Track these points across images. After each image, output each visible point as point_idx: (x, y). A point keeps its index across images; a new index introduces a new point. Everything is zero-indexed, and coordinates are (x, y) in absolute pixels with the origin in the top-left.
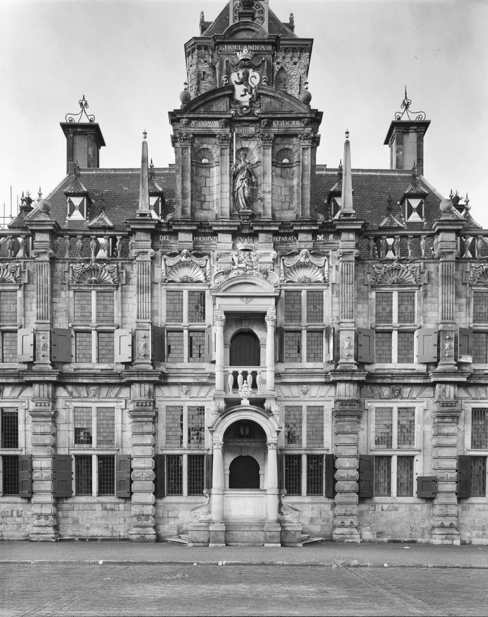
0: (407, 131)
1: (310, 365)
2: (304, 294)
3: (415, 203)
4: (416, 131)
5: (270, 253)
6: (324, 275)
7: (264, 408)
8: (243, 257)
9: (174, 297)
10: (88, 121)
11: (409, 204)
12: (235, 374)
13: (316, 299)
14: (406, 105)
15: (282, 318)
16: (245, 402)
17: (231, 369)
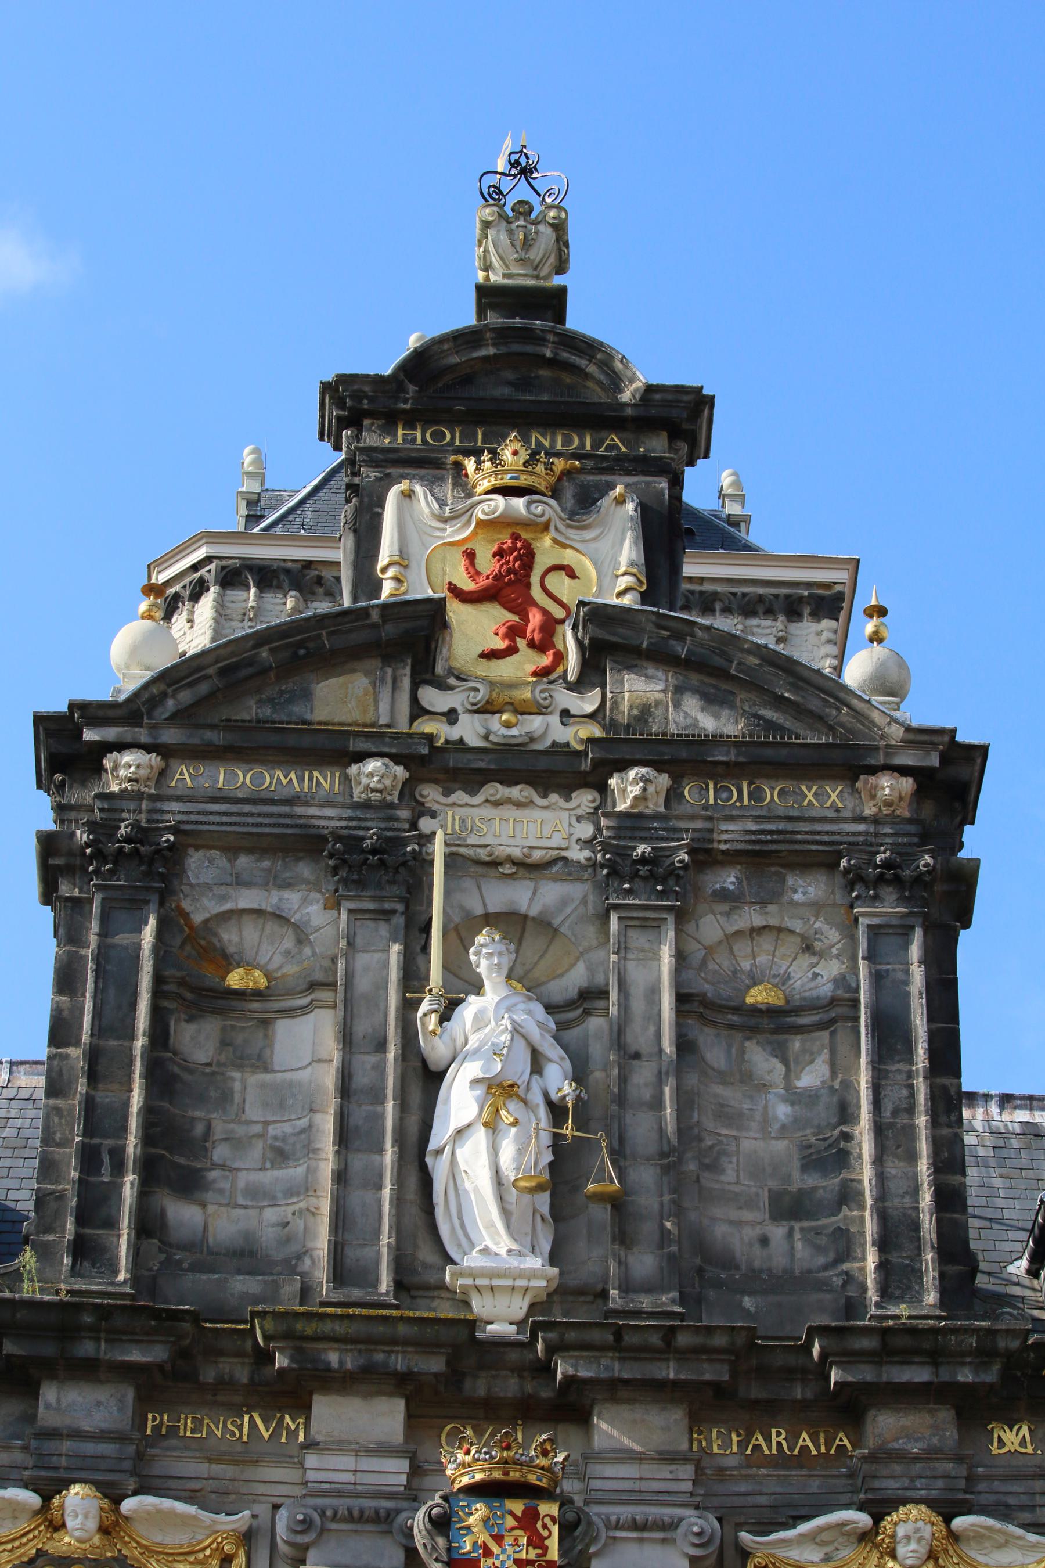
5: (672, 1525)
8: (483, 1537)
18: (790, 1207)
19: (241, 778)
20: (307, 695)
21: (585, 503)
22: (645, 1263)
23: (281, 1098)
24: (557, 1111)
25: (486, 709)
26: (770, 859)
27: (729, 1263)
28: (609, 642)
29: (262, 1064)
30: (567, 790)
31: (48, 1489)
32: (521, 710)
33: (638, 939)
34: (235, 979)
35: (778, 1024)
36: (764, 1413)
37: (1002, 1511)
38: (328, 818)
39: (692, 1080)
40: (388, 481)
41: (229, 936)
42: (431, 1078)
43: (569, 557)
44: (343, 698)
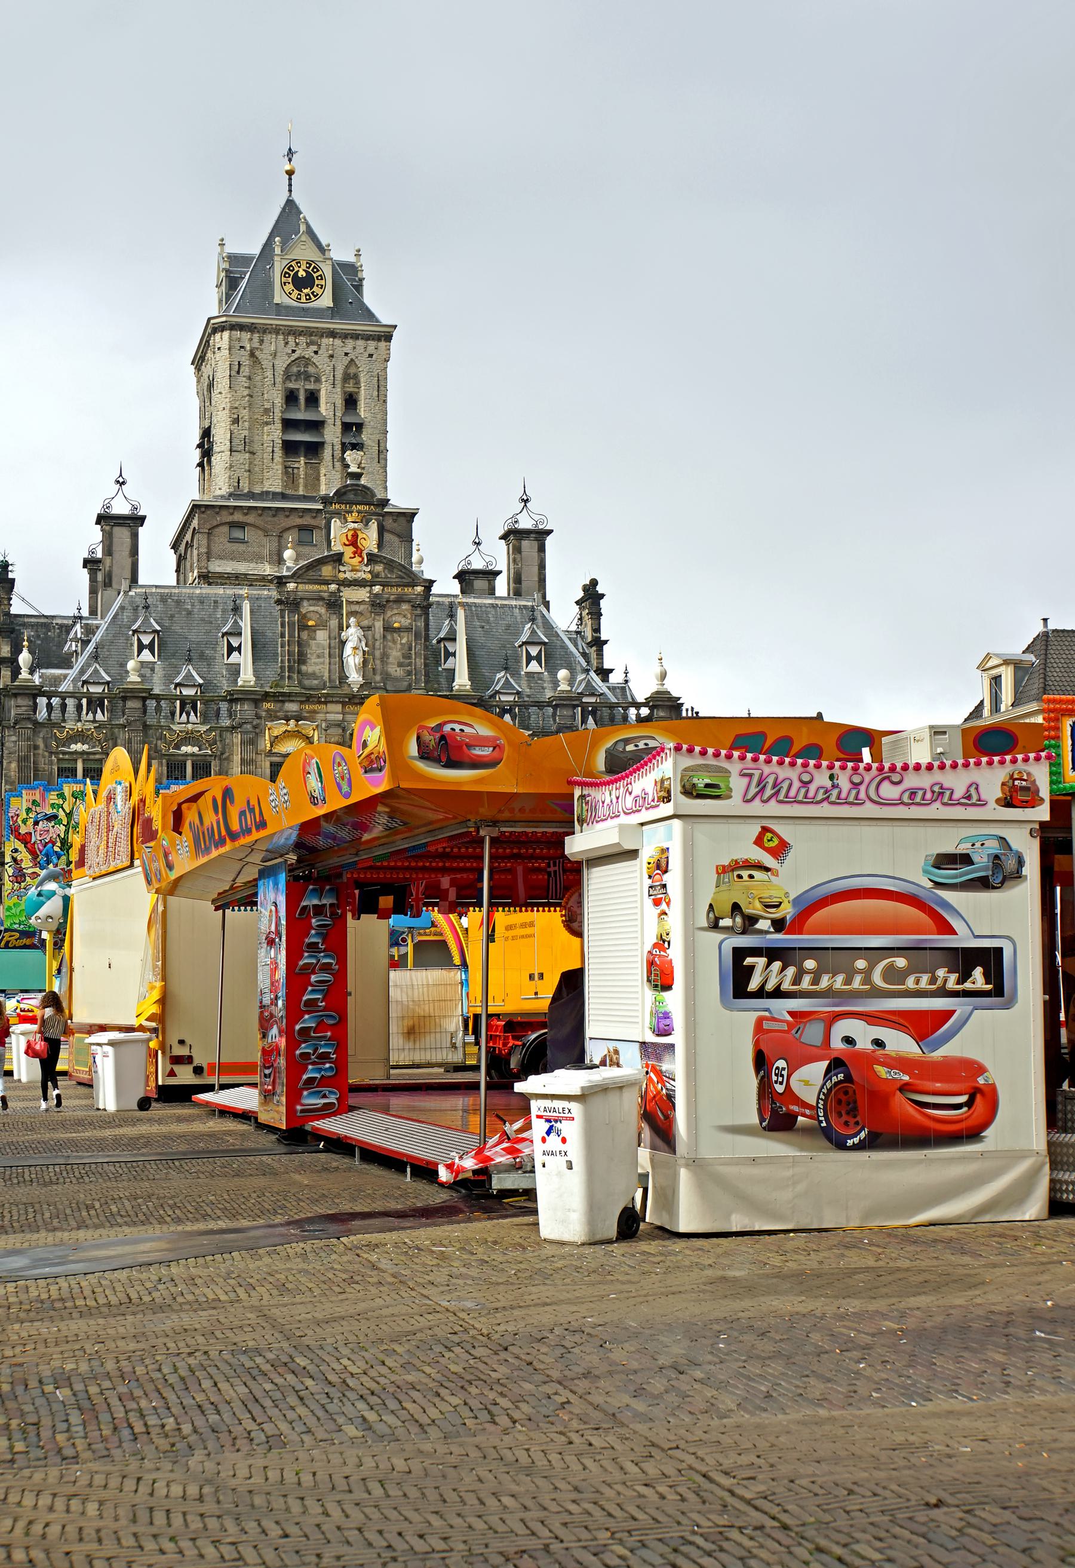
0: (527, 541)
3: (534, 651)
4: (536, 539)
11: (527, 650)
14: (526, 501)
18: (400, 665)
19: (310, 587)
20: (320, 570)
21: (367, 525)
22: (378, 678)
23: (318, 645)
26: (399, 600)
28: (372, 559)
30: (365, 586)
31: (288, 720)
34: (310, 623)
38: (325, 595)
42: (343, 643)
44: (327, 571)
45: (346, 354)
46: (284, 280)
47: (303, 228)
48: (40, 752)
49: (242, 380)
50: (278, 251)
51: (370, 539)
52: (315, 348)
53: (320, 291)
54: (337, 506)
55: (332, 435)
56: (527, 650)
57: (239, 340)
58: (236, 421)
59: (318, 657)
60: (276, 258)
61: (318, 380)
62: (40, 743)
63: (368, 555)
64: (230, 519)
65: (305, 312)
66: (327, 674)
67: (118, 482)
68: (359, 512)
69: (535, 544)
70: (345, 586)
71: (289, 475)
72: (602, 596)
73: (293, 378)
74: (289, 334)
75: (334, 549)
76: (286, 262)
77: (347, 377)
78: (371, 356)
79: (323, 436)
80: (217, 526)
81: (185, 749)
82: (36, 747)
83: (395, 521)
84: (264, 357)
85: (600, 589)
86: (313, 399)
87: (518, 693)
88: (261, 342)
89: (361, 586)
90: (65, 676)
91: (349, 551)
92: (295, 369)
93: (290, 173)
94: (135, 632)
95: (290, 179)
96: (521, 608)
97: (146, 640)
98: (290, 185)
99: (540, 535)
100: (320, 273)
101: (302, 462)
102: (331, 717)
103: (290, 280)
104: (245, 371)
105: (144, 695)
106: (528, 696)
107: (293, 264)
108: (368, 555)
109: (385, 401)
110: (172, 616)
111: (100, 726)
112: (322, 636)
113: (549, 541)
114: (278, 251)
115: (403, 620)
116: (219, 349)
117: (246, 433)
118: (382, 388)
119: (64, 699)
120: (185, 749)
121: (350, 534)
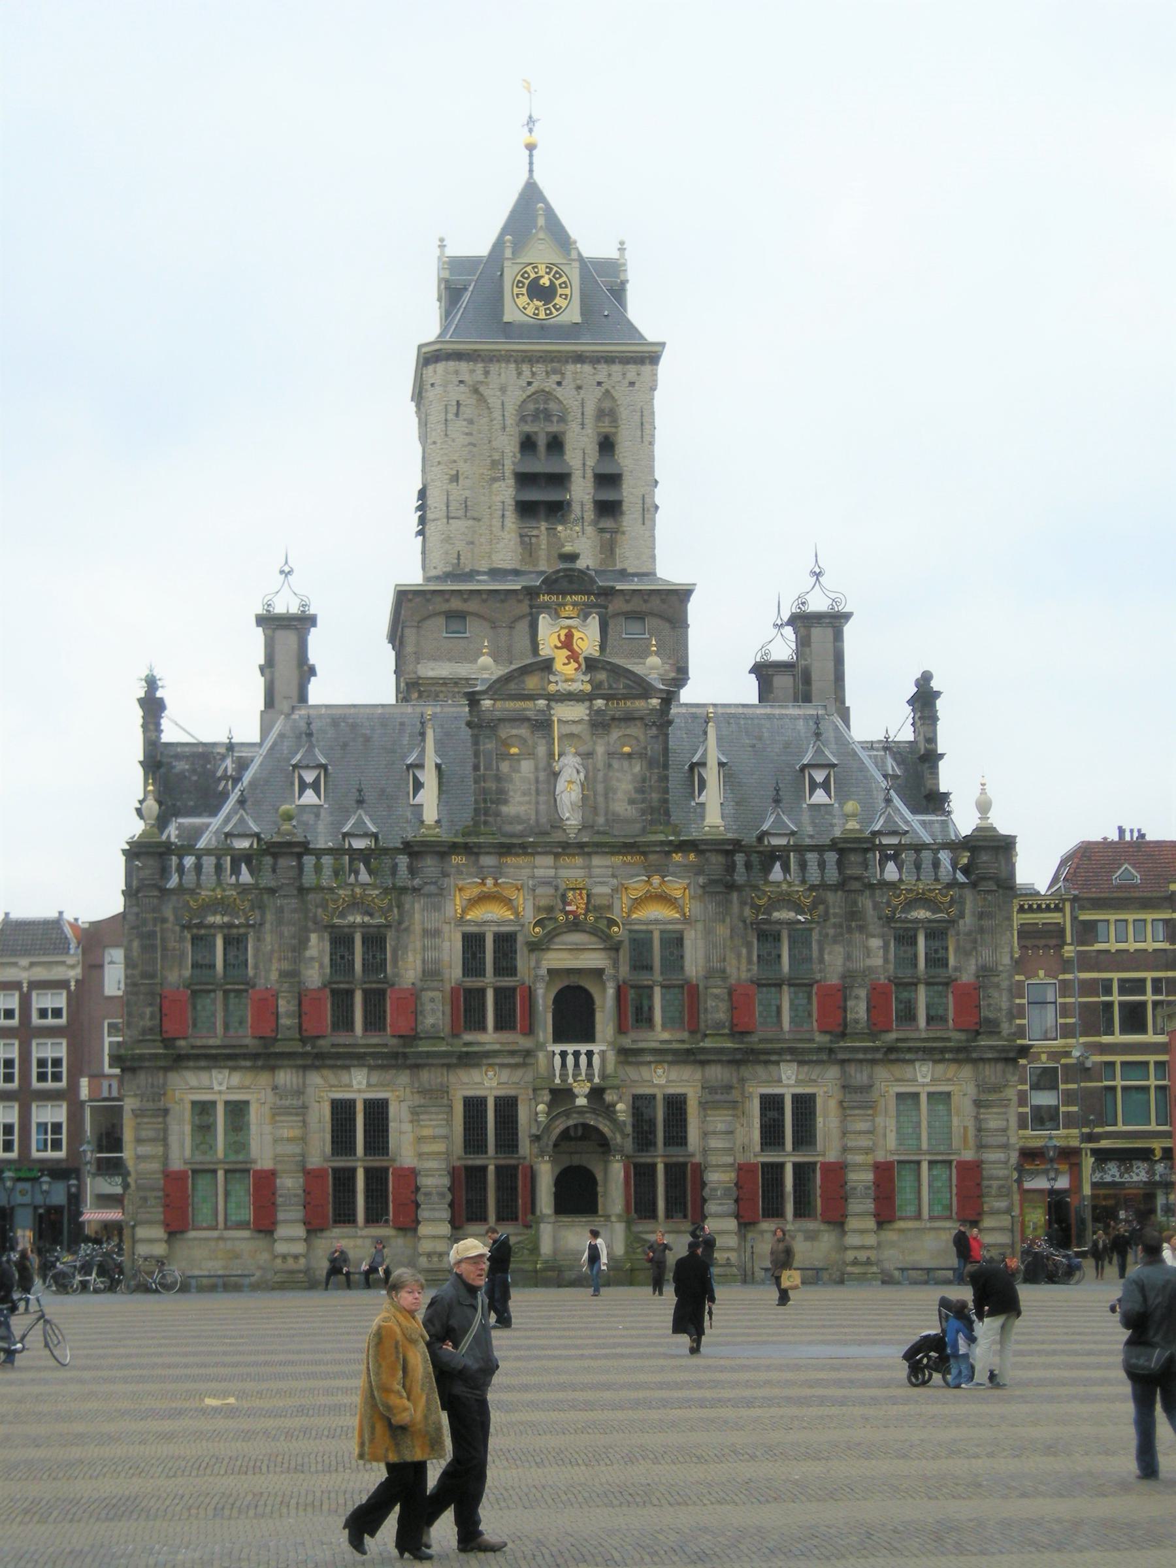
1: (666, 1036)
2: (656, 936)
3: (819, 776)
6: (683, 910)
7: (604, 1099)
9: (472, 943)
10: (294, 609)
11: (810, 776)
12: (564, 1054)
13: (675, 942)
14: (818, 575)
15: (624, 970)
16: (581, 1101)
17: (558, 1048)
18: (632, 802)
19: (511, 705)
20: (523, 682)
22: (601, 820)
24: (582, 785)
25: (566, 681)
26: (629, 718)
27: (619, 816)
28: (591, 665)
29: (519, 771)
30: (582, 701)
32: (573, 680)
33: (600, 741)
34: (514, 750)
35: (629, 756)
36: (624, 854)
37: (673, 874)
38: (529, 714)
39: (611, 774)
40: (539, 614)
41: (509, 741)
42: (556, 775)
43: (582, 635)
44: (532, 683)
45: (599, 384)
46: (516, 290)
47: (541, 222)
48: (169, 925)
49: (461, 424)
50: (508, 253)
51: (588, 640)
52: (557, 378)
53: (564, 303)
54: (546, 598)
55: (581, 492)
56: (810, 775)
57: (457, 372)
58: (455, 478)
59: (524, 794)
60: (507, 264)
61: (562, 419)
62: (168, 913)
63: (586, 659)
64: (445, 607)
65: (542, 330)
66: (533, 817)
67: (282, 572)
68: (574, 604)
69: (829, 632)
70: (557, 701)
71: (528, 546)
72: (937, 694)
73: (529, 419)
74: (523, 361)
75: (541, 653)
76: (517, 268)
77: (601, 414)
78: (632, 384)
79: (568, 490)
80: (429, 617)
81: (351, 919)
82: (164, 920)
83: (663, 601)
84: (491, 393)
85: (935, 685)
86: (556, 444)
87: (793, 833)
88: (487, 373)
89: (578, 701)
90: (208, 825)
91: (561, 656)
92: (531, 406)
93: (531, 147)
94: (295, 766)
95: (531, 156)
96: (806, 718)
97: (309, 777)
98: (531, 163)
99: (835, 621)
100: (564, 279)
101: (543, 528)
102: (539, 872)
103: (524, 290)
104: (467, 412)
105: (301, 849)
106: (811, 837)
107: (529, 269)
108: (586, 659)
109: (651, 443)
110: (345, 746)
111: (244, 889)
112: (526, 766)
113: (849, 630)
114: (508, 253)
115: (634, 742)
116: (432, 385)
117: (467, 493)
118: (646, 426)
119: (199, 858)
120: (351, 919)
121: (563, 633)
